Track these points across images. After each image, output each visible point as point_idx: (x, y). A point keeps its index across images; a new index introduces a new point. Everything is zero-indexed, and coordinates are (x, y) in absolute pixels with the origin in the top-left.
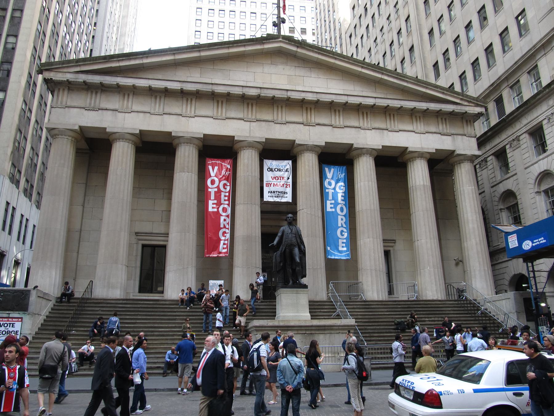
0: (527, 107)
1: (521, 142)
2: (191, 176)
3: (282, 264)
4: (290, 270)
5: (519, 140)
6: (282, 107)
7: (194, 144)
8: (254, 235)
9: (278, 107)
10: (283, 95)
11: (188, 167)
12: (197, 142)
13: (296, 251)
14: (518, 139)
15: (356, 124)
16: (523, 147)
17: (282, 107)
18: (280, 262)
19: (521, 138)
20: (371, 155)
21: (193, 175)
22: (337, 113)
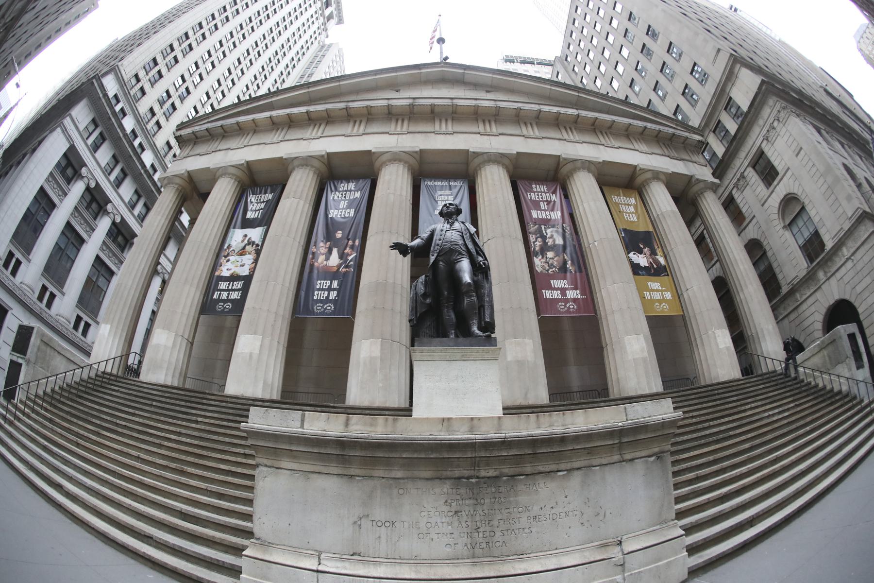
0: (735, 143)
1: (748, 179)
2: (298, 202)
3: (428, 301)
4: (453, 316)
5: (744, 177)
6: (446, 120)
7: (312, 166)
8: (392, 280)
9: (441, 120)
10: (449, 102)
11: (295, 192)
12: (317, 163)
13: (465, 265)
14: (742, 176)
15: (559, 136)
16: (751, 183)
17: (446, 120)
18: (425, 295)
19: (746, 174)
20: (589, 171)
21: (302, 202)
22: (529, 126)
